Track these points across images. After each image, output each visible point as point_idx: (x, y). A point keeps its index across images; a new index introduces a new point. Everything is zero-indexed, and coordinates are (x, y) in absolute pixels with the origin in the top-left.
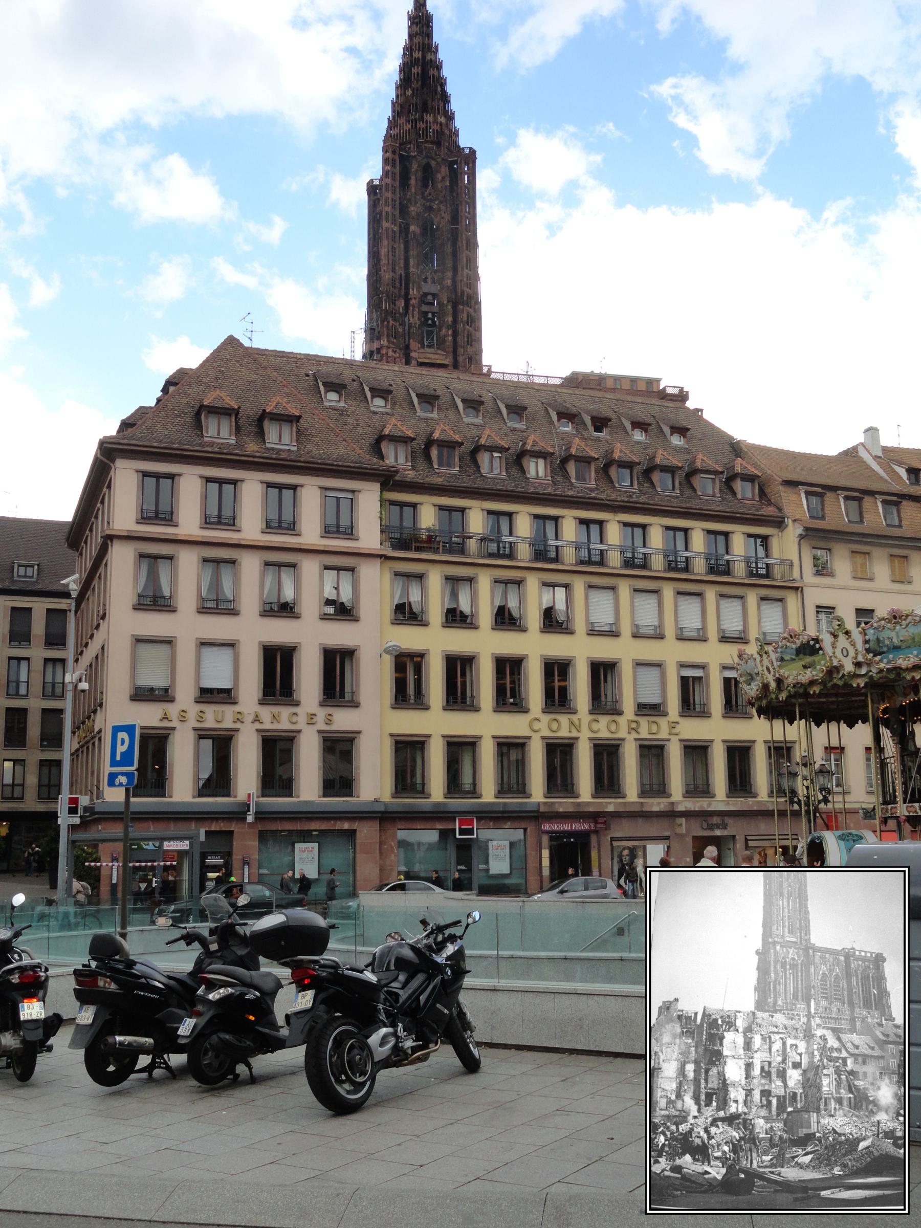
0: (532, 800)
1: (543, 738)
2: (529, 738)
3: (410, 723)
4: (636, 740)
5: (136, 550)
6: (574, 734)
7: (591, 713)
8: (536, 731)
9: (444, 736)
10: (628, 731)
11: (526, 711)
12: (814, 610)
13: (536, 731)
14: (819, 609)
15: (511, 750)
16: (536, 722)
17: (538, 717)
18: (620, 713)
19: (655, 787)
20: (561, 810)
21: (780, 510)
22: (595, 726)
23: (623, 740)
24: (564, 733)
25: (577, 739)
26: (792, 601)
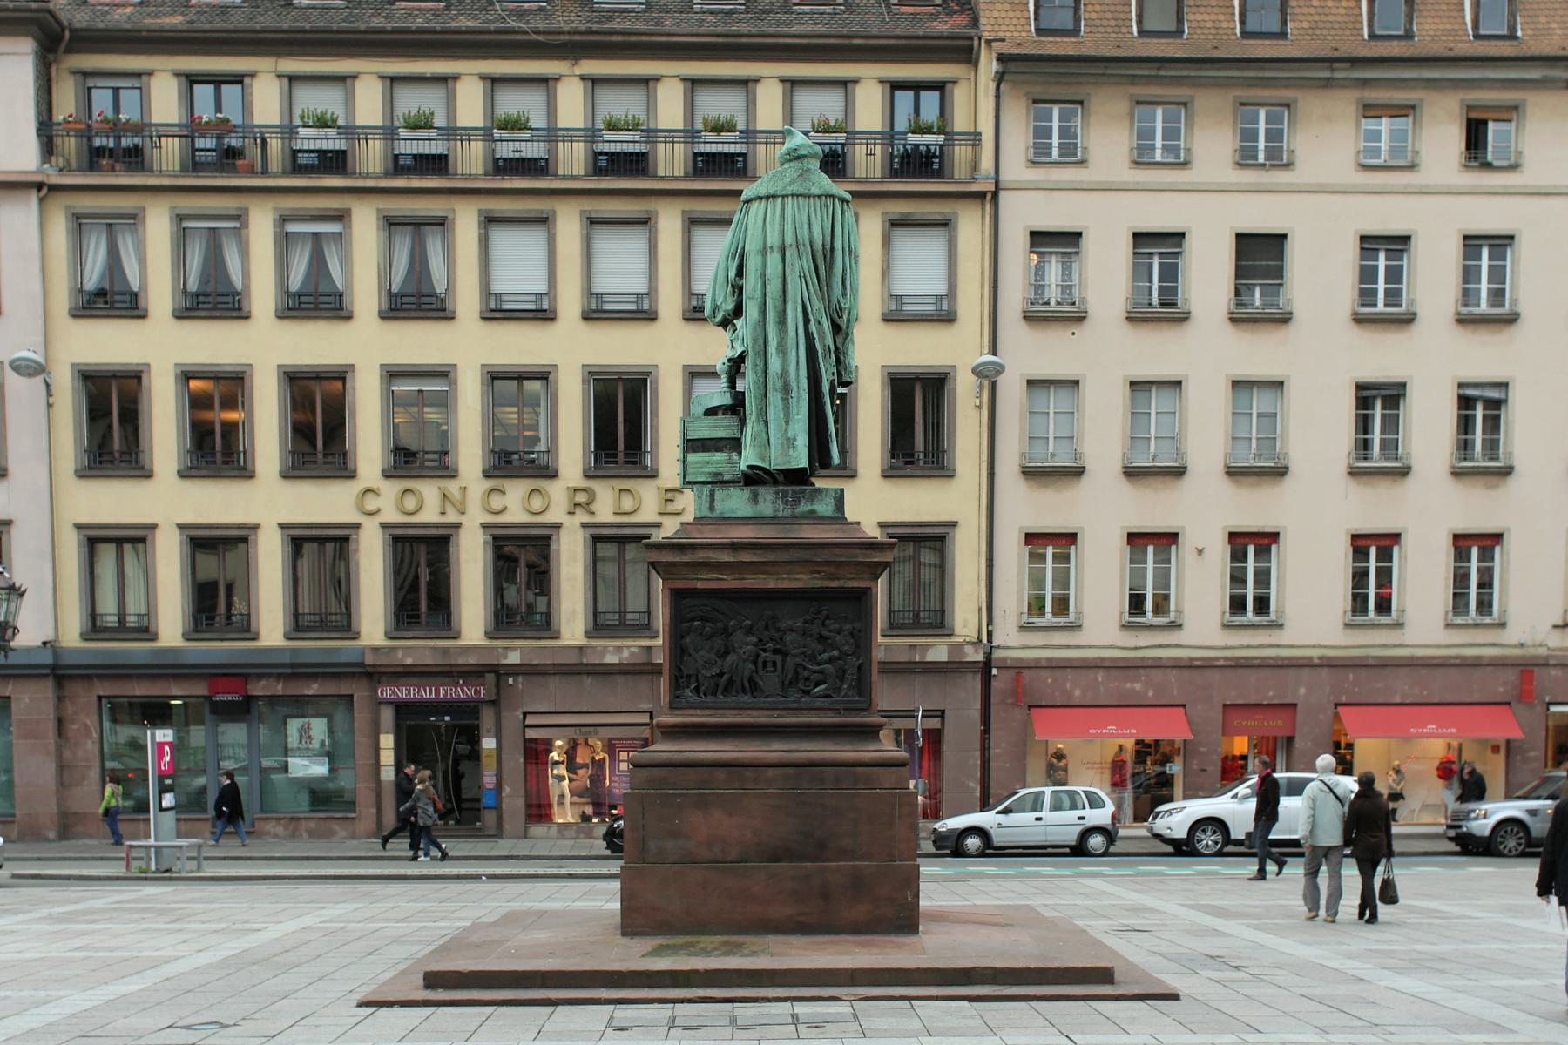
0: (464, 641)
1: (385, 526)
2: (357, 526)
3: (113, 502)
4: (584, 525)
5: (378, 210)
6: (452, 517)
7: (487, 475)
8: (371, 514)
9: (182, 527)
10: (472, 506)
11: (352, 475)
12: (1023, 240)
13: (371, 514)
14: (1039, 238)
15: (320, 551)
16: (369, 496)
17: (373, 485)
18: (550, 473)
19: (132, 621)
20: (409, 661)
21: (975, 22)
22: (497, 502)
23: (557, 526)
24: (430, 515)
25: (457, 526)
26: (970, 226)
